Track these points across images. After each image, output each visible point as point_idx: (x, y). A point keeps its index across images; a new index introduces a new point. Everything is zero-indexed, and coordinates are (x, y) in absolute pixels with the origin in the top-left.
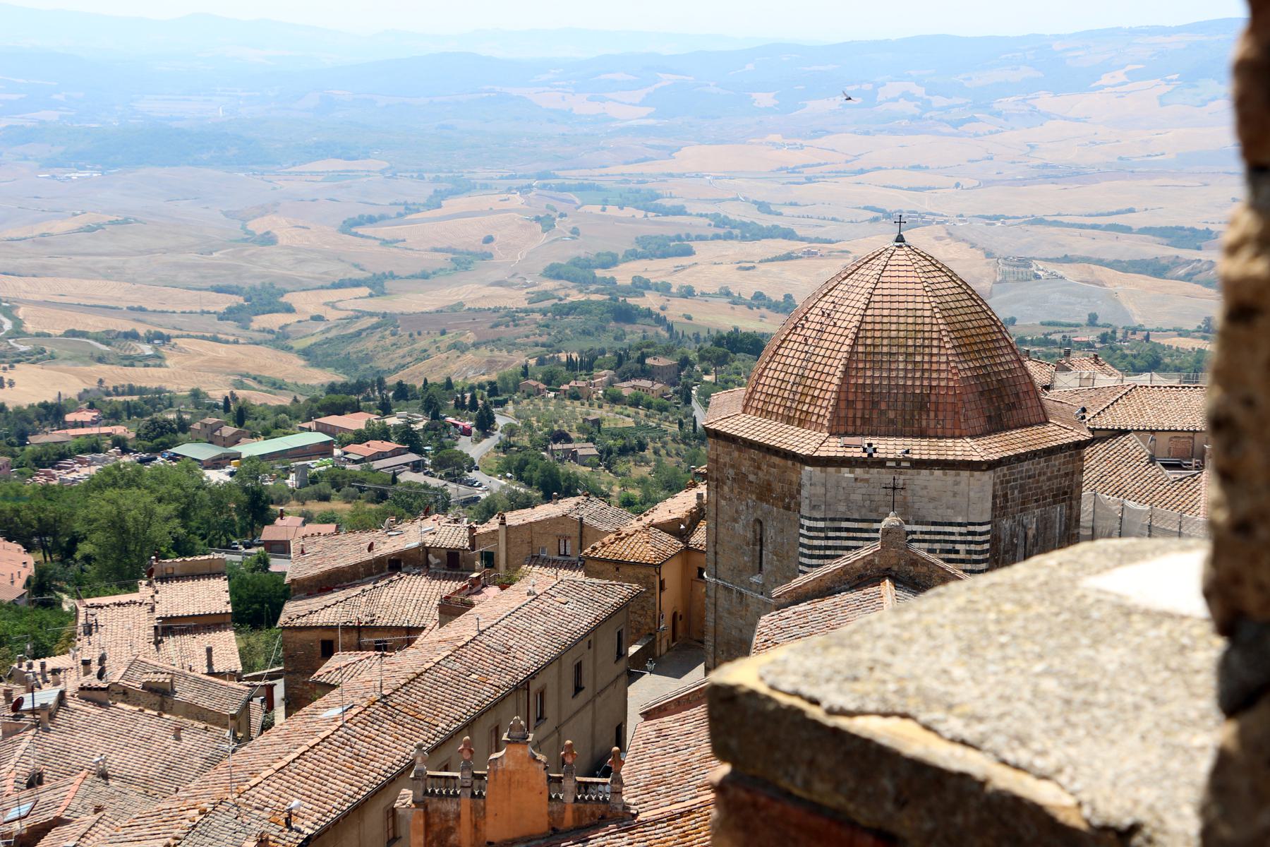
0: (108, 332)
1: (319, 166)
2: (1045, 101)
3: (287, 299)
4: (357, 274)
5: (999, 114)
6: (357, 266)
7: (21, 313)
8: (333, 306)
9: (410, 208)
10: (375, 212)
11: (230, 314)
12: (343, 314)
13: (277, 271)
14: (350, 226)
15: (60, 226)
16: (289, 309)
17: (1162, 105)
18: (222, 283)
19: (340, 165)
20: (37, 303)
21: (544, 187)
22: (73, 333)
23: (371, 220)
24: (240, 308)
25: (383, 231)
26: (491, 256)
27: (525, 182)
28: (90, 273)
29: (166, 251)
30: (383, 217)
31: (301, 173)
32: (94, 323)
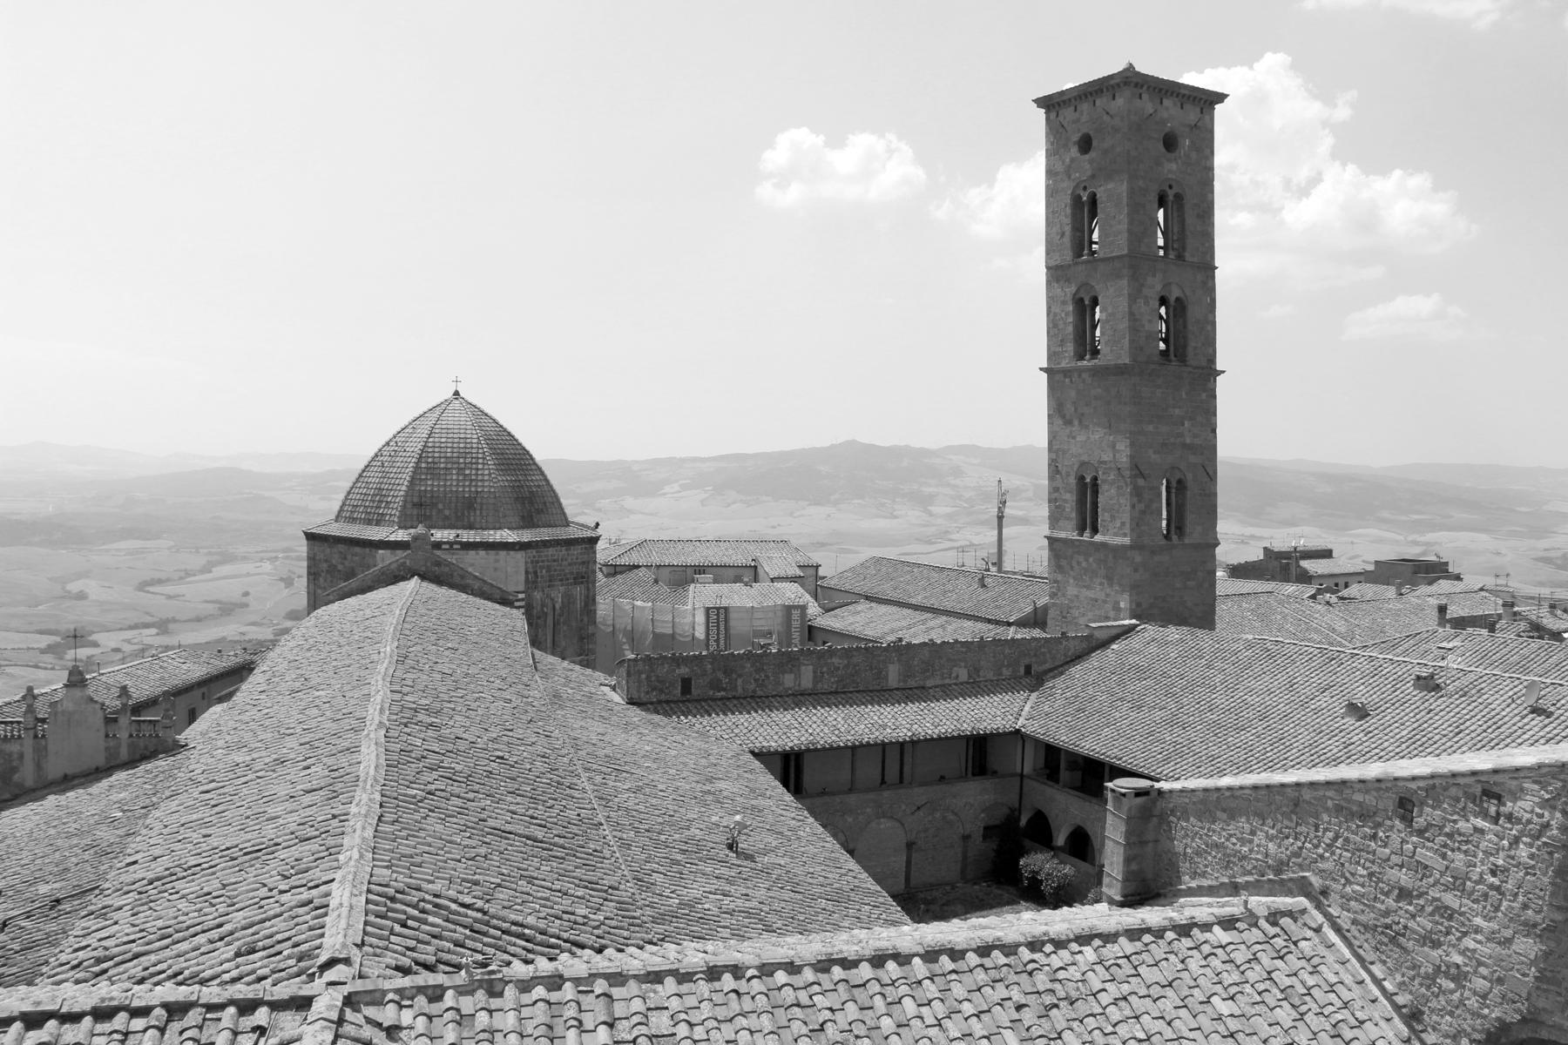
1: (123, 545)
2: (629, 502)
3: (94, 637)
4: (148, 619)
5: (599, 510)
8: (128, 641)
9: (188, 574)
10: (163, 576)
11: (50, 649)
14: (143, 586)
16: (95, 645)
18: (43, 627)
19: (138, 544)
21: (287, 558)
23: (160, 582)
25: (169, 589)
26: (247, 605)
31: (107, 550)
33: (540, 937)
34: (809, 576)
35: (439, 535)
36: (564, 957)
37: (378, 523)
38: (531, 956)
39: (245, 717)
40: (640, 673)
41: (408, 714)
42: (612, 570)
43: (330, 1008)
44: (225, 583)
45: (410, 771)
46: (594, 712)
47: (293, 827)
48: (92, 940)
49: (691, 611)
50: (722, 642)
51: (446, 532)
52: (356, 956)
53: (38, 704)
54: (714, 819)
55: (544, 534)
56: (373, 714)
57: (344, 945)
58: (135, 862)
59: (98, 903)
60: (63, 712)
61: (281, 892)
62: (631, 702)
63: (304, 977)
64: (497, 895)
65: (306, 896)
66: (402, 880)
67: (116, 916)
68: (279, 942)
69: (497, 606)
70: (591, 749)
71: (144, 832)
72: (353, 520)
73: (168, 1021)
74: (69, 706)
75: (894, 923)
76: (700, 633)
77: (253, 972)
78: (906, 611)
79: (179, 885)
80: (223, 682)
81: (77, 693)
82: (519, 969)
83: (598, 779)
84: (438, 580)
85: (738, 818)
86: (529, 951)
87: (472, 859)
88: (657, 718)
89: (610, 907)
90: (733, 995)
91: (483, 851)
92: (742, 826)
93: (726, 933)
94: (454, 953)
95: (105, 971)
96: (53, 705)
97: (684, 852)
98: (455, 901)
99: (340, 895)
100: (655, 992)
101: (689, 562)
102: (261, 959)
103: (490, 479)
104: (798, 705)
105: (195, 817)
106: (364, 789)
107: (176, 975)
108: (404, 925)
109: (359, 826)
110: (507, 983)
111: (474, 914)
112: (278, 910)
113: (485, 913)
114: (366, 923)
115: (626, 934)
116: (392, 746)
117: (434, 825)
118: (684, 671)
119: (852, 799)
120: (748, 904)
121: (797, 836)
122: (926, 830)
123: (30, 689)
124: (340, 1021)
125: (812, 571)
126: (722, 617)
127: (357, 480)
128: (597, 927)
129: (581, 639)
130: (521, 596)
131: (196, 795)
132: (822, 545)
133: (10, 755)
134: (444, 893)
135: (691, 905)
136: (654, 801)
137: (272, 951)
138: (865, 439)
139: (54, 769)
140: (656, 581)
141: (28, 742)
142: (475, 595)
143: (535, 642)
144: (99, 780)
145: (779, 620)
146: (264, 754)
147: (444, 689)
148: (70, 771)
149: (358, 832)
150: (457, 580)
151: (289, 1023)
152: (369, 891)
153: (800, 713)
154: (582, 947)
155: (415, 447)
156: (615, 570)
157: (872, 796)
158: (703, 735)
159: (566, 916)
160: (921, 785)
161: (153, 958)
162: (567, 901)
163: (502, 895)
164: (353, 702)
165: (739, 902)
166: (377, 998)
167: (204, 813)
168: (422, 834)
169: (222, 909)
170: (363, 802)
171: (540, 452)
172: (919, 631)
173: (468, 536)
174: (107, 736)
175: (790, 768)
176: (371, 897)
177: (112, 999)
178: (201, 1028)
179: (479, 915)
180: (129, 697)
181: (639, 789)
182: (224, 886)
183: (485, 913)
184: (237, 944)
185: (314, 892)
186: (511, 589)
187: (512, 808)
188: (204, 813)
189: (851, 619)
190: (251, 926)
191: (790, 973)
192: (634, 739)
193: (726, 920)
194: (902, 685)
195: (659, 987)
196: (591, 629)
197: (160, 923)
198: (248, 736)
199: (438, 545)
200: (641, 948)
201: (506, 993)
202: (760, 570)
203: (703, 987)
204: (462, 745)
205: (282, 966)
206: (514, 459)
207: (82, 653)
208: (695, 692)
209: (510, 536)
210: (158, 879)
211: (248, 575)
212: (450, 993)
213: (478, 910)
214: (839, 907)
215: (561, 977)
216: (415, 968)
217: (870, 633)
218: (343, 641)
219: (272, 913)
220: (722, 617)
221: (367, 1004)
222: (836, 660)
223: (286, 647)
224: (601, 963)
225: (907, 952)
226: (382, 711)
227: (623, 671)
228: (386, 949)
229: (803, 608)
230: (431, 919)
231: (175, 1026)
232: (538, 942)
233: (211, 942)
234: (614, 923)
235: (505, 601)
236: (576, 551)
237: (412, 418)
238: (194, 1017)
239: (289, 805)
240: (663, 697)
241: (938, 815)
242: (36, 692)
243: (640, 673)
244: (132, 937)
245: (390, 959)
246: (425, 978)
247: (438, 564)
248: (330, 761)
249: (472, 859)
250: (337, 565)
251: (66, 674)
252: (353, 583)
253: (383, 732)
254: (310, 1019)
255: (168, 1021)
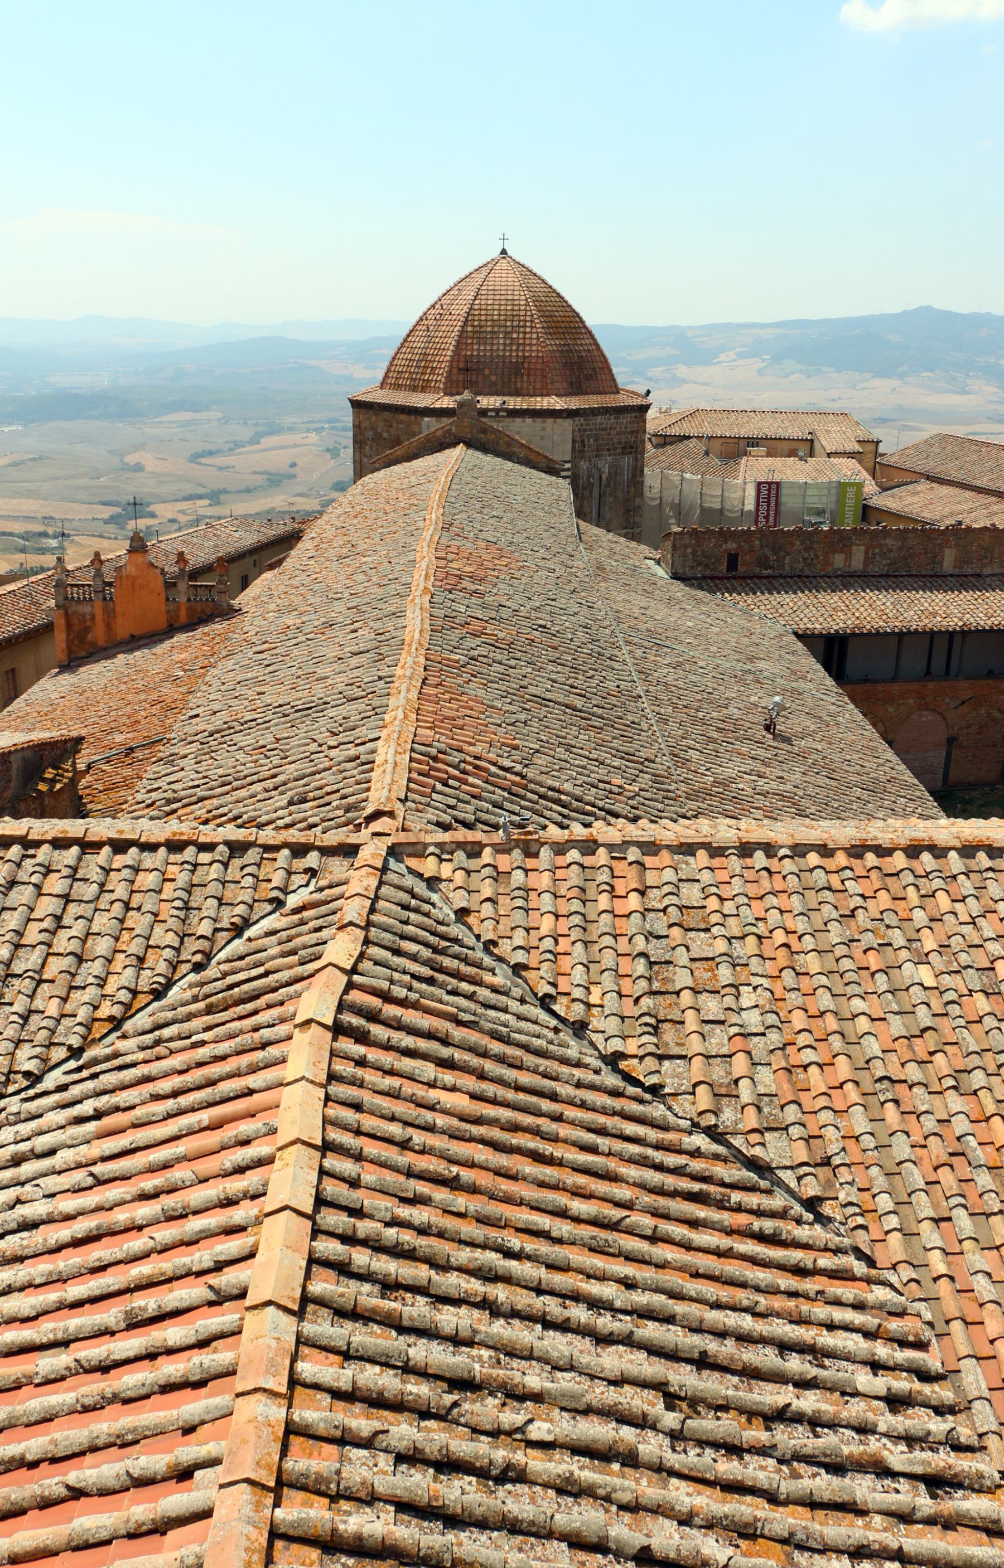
0: (27, 533)
2: (682, 371)
5: (650, 379)
6: (200, 485)
9: (237, 445)
11: (112, 520)
12: (190, 518)
13: (145, 490)
14: (196, 457)
17: (760, 375)
18: (105, 498)
19: (188, 416)
21: (333, 428)
23: (211, 453)
25: (219, 461)
27: (318, 425)
30: (218, 452)
31: (161, 423)
33: (575, 804)
34: (867, 452)
35: (487, 402)
36: (598, 824)
37: (423, 390)
38: (566, 822)
39: (295, 582)
40: (686, 547)
41: (453, 580)
42: (661, 440)
43: (374, 856)
44: (273, 454)
45: (454, 636)
46: (637, 584)
47: (341, 687)
48: (161, 783)
49: (741, 487)
50: (771, 519)
51: (492, 399)
52: (400, 809)
53: (105, 569)
54: (753, 699)
55: (593, 401)
56: (420, 579)
57: (388, 799)
58: (197, 716)
59: (164, 751)
60: (127, 576)
61: (330, 748)
62: (675, 576)
63: (351, 827)
64: (535, 760)
65: (353, 751)
66: (443, 741)
67: (182, 763)
68: (328, 794)
69: (543, 475)
70: (633, 622)
71: (204, 688)
72: (398, 387)
73: (230, 858)
74: (131, 570)
75: (928, 818)
76: (750, 506)
77: (305, 819)
78: (968, 494)
79: (237, 738)
80: (273, 550)
81: (139, 558)
82: (554, 832)
83: (639, 653)
84: (484, 448)
85: (777, 699)
86: (564, 816)
87: (513, 724)
88: (700, 594)
89: (645, 780)
90: (764, 873)
91: (523, 717)
92: (781, 707)
93: (759, 814)
94: (493, 813)
95: (175, 811)
96: (118, 569)
97: (719, 730)
98: (494, 764)
99: (385, 752)
100: (687, 863)
101: (743, 433)
102: (312, 808)
103: (537, 342)
104: (847, 587)
105: (250, 675)
106: (409, 652)
107: (235, 819)
108: (445, 784)
109: (404, 687)
110: (543, 844)
111: (513, 777)
112: (327, 764)
113: (523, 777)
114: (409, 780)
115: (660, 806)
116: (437, 612)
117: (474, 688)
118: (731, 546)
119: (896, 688)
120: (782, 787)
121: (837, 723)
122: (969, 726)
123: (97, 554)
124: (384, 869)
125: (871, 447)
126: (773, 492)
127: (402, 346)
128: (632, 798)
129: (627, 511)
130: (568, 466)
131: (250, 655)
132: (882, 421)
133: (84, 615)
134: (484, 755)
135: (725, 783)
136: (694, 678)
137: (321, 801)
138: (939, 305)
139: (122, 630)
140: (707, 453)
141: (99, 604)
142: (519, 462)
143: (581, 514)
144: (162, 641)
145: (833, 499)
146: (313, 617)
147: (488, 557)
148: (136, 633)
149: (403, 693)
150: (503, 447)
151: (337, 867)
152: (412, 750)
153: (846, 595)
154: (617, 816)
155: (460, 310)
156: (665, 441)
157: (914, 686)
158: (747, 613)
159: (601, 785)
160: (968, 678)
161: (215, 802)
162: (603, 771)
163: (540, 760)
164: (398, 568)
165: (774, 785)
166: (419, 850)
167: (259, 672)
168: (464, 698)
169: (276, 761)
170: (409, 665)
171: (593, 315)
172: (977, 513)
173: (514, 403)
174: (167, 600)
175: (833, 651)
176: (414, 755)
177: (182, 834)
178: (259, 866)
179: (518, 779)
180: (186, 562)
181: (679, 665)
182: (278, 740)
183: (523, 777)
184: (290, 793)
185: (361, 748)
186: (557, 458)
187: (553, 676)
188: (259, 672)
189: (909, 500)
190: (302, 778)
191: (822, 856)
192: (676, 614)
193: (760, 801)
194: (956, 571)
195: (691, 859)
196: (638, 500)
197: (221, 772)
198: (297, 600)
199: (484, 412)
200: (675, 821)
201: (542, 854)
202: (817, 446)
203: (734, 863)
204: (505, 613)
205: (331, 815)
206: (563, 322)
207: (142, 523)
208: (741, 569)
209: (557, 403)
210: (218, 732)
211: (295, 446)
212: (488, 850)
213: (516, 774)
214: (875, 795)
215: (595, 842)
216: (455, 825)
217: (927, 515)
218: (388, 508)
219: (321, 766)
220: (773, 492)
221: (409, 855)
222: (889, 542)
223: (333, 515)
224: (634, 832)
225: (943, 844)
226: (427, 577)
227: (669, 544)
228: (428, 805)
229: (860, 486)
230: (471, 779)
231: (237, 862)
232: (573, 808)
233: (267, 791)
234: (648, 795)
235: (552, 470)
236: (625, 419)
237: (456, 279)
238: (252, 855)
239: (338, 667)
240: (708, 573)
241: (983, 711)
242: (103, 557)
243: (686, 547)
244: (196, 783)
245: (431, 815)
246: (462, 834)
247: (484, 431)
248: (377, 625)
249: (513, 724)
250: (383, 433)
251: (127, 544)
252: (399, 451)
253: (428, 597)
254: (356, 865)
255: (230, 858)
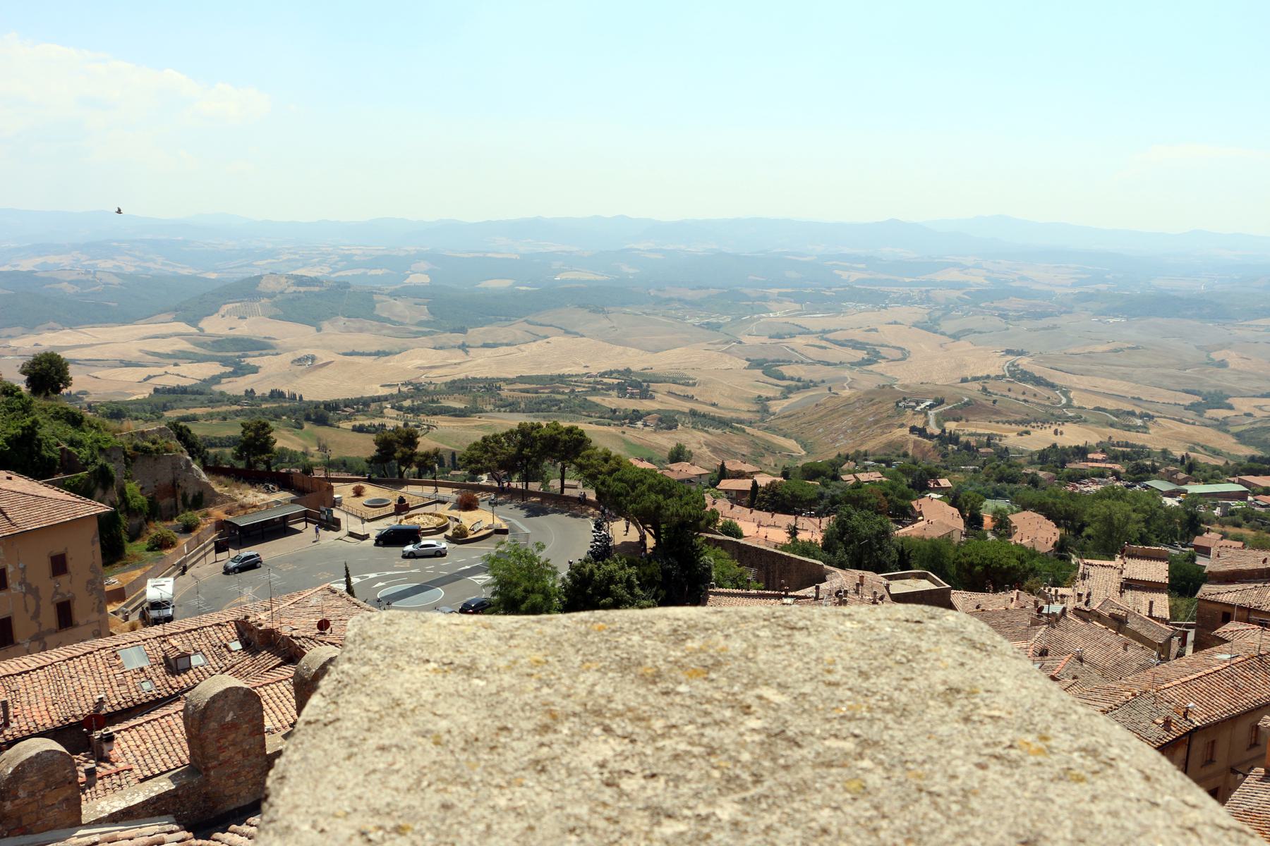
3: (1230, 401)
7: (1072, 395)
8: (1260, 408)
11: (1192, 407)
15: (1100, 348)
16: (1230, 407)
18: (1189, 388)
20: (1081, 390)
22: (1098, 409)
24: (1199, 404)
28: (1112, 376)
29: (1158, 366)
32: (1111, 404)
